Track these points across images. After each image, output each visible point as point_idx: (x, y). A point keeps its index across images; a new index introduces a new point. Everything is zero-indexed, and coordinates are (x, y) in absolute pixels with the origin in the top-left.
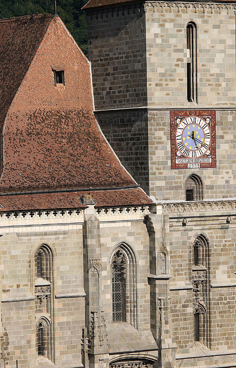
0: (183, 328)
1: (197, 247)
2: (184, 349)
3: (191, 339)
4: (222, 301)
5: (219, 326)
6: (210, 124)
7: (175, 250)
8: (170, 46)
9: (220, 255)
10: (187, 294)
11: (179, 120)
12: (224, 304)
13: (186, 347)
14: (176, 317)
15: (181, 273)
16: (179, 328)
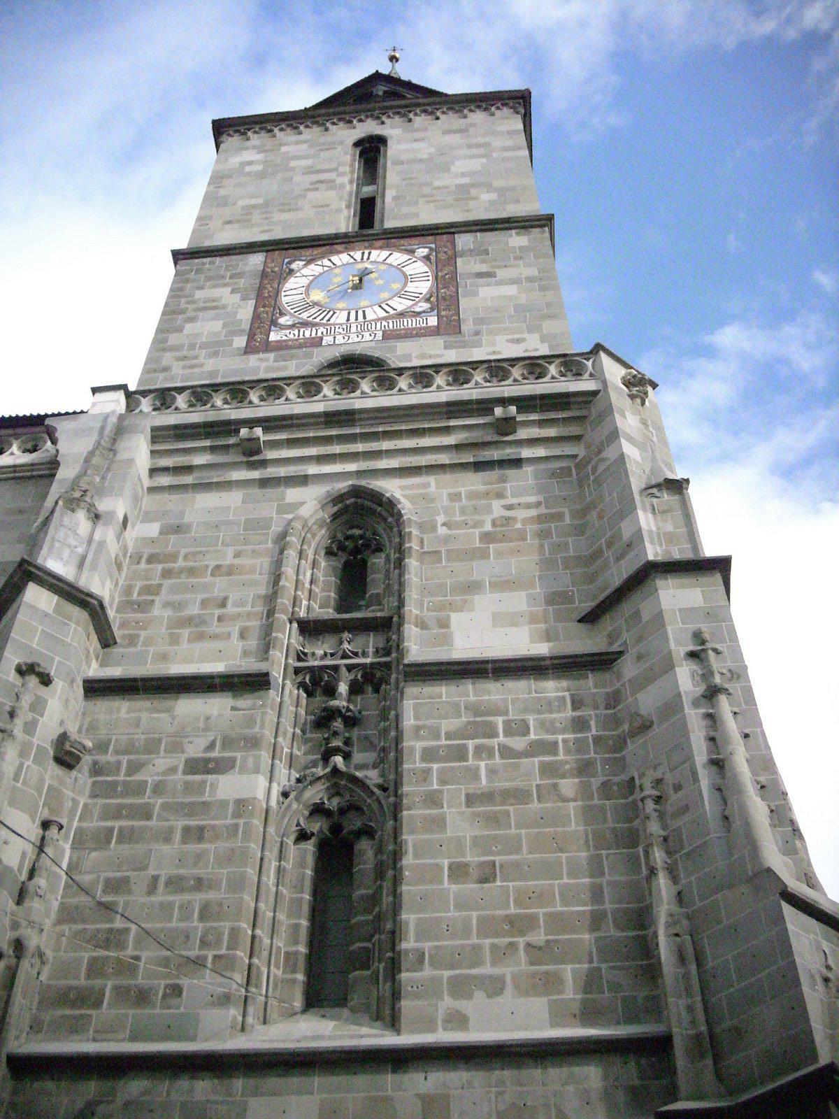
0: (175, 884)
1: (364, 563)
2: (157, 1011)
3: (223, 951)
4: (494, 742)
5: (467, 873)
6: (433, 258)
7: (199, 549)
8: (293, 169)
9: (484, 555)
10: (233, 709)
11: (294, 266)
12: (506, 752)
13: (175, 1001)
14: (131, 816)
15: (218, 631)
16: (139, 880)
